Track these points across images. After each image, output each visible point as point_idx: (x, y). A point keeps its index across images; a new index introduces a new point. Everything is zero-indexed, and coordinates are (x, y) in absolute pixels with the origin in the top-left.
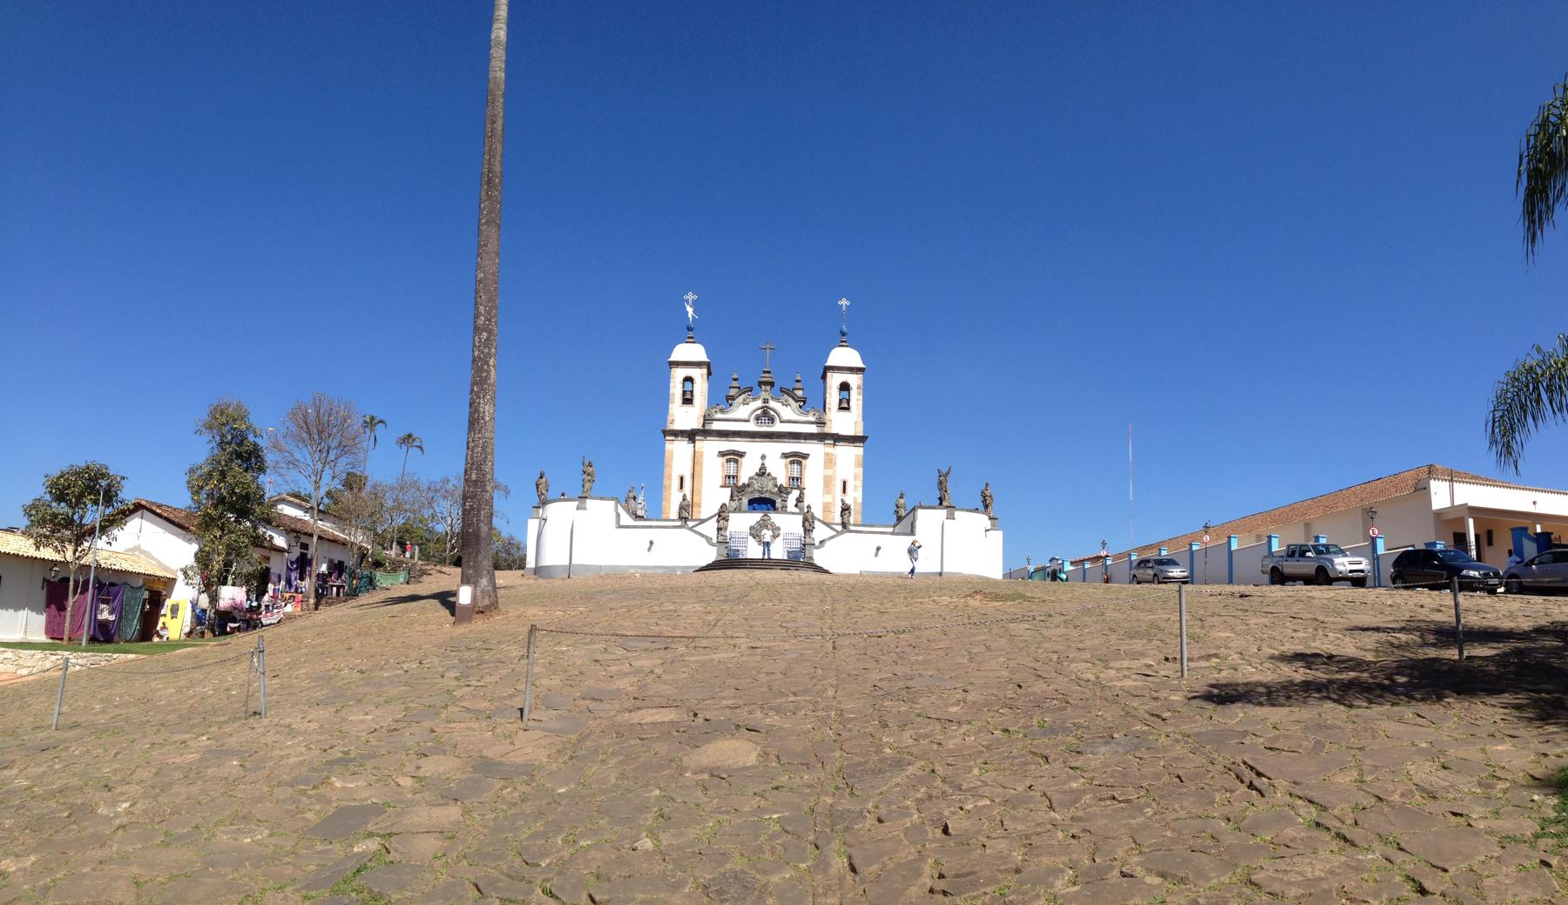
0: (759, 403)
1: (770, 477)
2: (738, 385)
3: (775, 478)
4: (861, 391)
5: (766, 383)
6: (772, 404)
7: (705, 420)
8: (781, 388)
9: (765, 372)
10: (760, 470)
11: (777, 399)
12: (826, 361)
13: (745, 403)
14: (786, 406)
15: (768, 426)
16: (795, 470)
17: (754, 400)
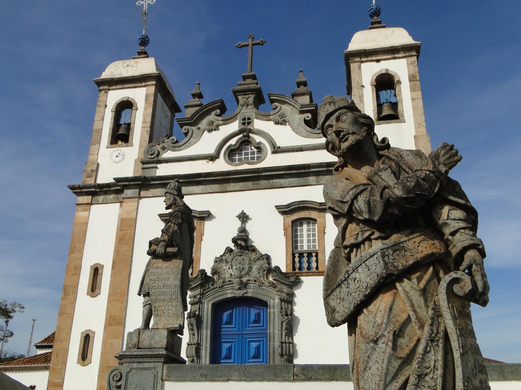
0: (234, 126)
1: (253, 256)
2: (199, 103)
3: (268, 258)
4: (418, 82)
5: (244, 92)
6: (258, 124)
7: (143, 163)
8: (269, 95)
9: (245, 78)
10: (234, 241)
11: (266, 117)
12: (347, 47)
13: (213, 128)
14: (281, 124)
15: (249, 164)
16: (305, 238)
17: (226, 122)
